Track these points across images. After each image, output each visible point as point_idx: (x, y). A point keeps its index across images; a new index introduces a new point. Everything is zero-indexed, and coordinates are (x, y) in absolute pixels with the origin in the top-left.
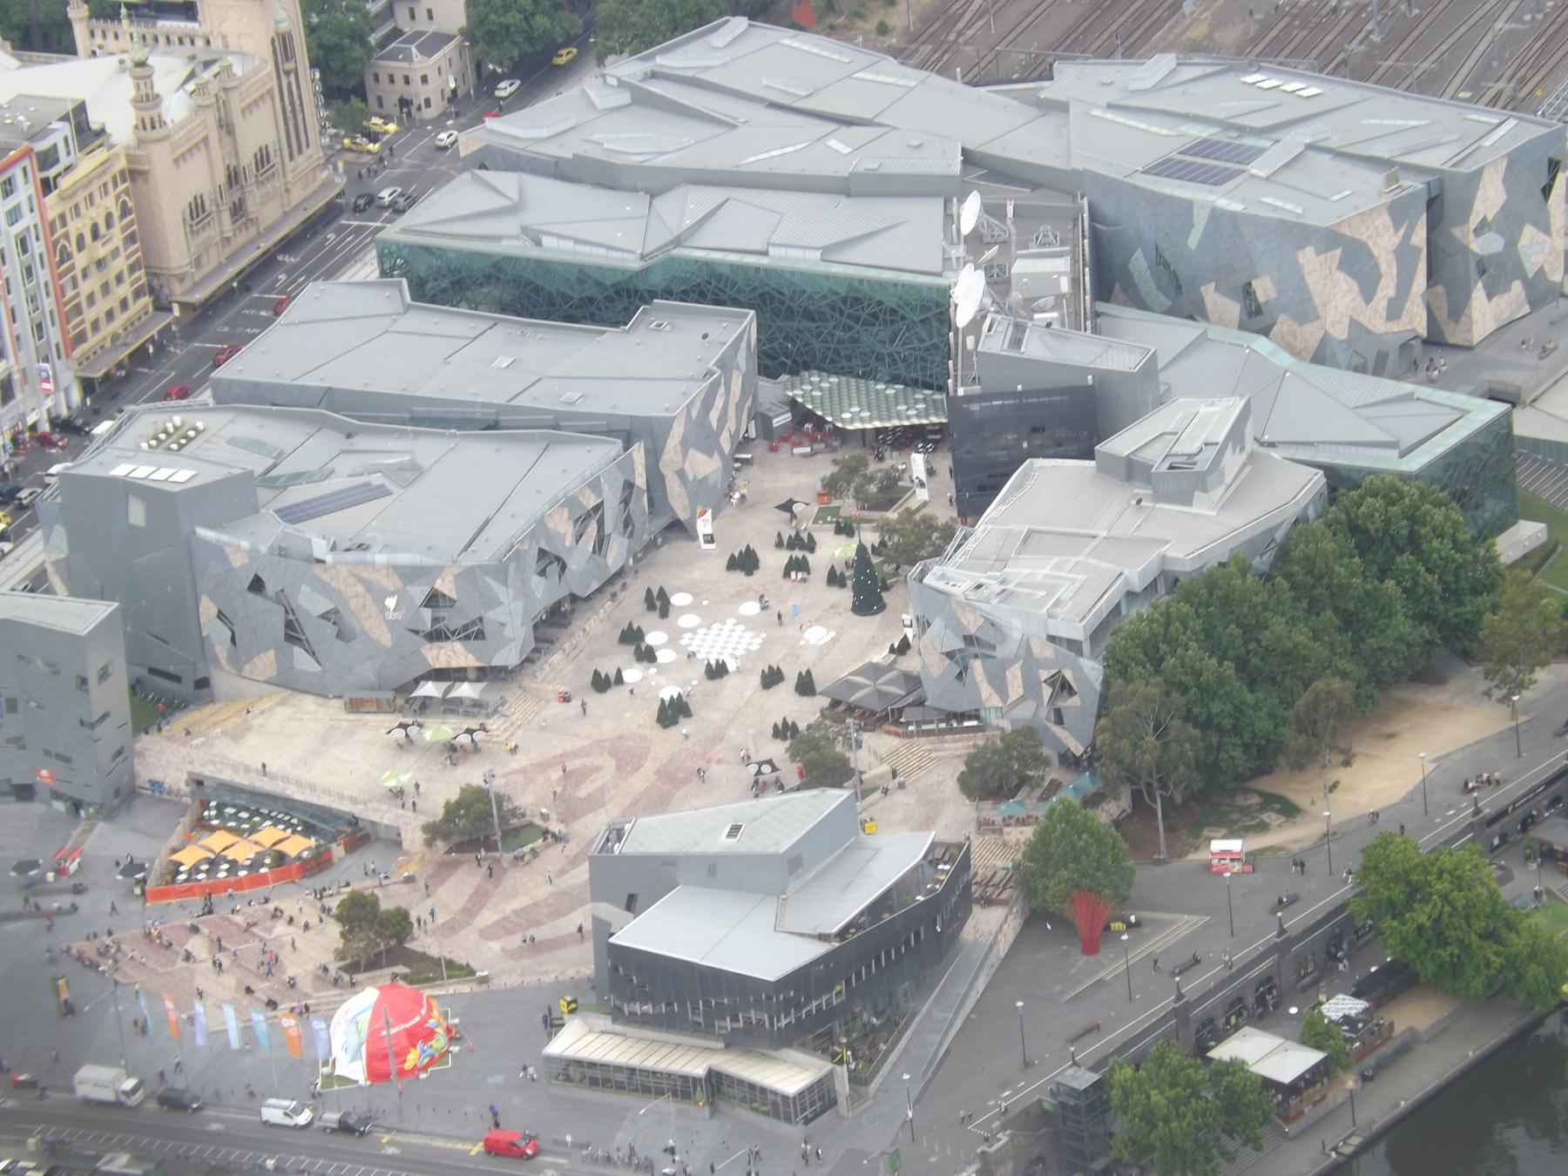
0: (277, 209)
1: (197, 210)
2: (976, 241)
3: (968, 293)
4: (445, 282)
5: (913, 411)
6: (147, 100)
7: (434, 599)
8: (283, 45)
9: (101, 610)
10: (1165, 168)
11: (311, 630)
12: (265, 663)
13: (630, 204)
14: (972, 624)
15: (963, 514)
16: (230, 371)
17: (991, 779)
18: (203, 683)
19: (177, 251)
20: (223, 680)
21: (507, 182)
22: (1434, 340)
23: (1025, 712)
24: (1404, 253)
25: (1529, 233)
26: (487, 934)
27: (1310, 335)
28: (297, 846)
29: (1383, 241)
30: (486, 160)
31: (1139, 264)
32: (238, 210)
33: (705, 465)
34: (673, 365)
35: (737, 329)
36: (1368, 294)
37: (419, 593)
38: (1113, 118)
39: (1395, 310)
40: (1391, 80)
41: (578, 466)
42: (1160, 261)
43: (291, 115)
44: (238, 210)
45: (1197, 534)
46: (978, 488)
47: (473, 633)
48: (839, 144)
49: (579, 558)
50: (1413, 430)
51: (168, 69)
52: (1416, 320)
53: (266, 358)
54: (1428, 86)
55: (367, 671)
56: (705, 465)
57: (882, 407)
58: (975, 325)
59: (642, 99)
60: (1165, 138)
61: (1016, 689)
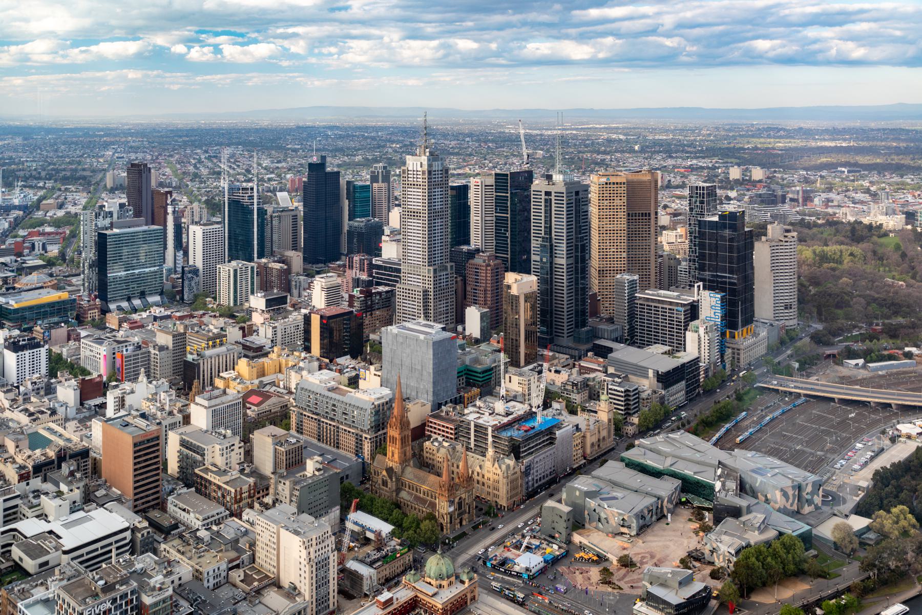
0: (605, 446)
1: (593, 445)
2: (720, 477)
3: (718, 485)
5: (706, 505)
7: (623, 519)
8: (609, 420)
9: (569, 509)
10: (753, 471)
11: (602, 520)
14: (715, 546)
15: (714, 524)
17: (715, 575)
19: (588, 451)
20: (587, 525)
21: (643, 450)
22: (798, 512)
23: (722, 564)
24: (794, 495)
25: (816, 497)
26: (626, 583)
27: (777, 506)
29: (790, 492)
31: (747, 486)
34: (666, 488)
36: (787, 499)
37: (621, 518)
38: (744, 461)
39: (792, 505)
40: (791, 463)
41: (650, 501)
42: (751, 487)
43: (609, 432)
45: (754, 537)
46: (717, 521)
47: (629, 527)
48: (698, 455)
49: (648, 518)
50: (795, 528)
52: (795, 508)
53: (600, 472)
54: (798, 466)
55: (610, 530)
56: (671, 506)
57: (700, 502)
58: (719, 491)
60: (753, 466)
61: (721, 560)
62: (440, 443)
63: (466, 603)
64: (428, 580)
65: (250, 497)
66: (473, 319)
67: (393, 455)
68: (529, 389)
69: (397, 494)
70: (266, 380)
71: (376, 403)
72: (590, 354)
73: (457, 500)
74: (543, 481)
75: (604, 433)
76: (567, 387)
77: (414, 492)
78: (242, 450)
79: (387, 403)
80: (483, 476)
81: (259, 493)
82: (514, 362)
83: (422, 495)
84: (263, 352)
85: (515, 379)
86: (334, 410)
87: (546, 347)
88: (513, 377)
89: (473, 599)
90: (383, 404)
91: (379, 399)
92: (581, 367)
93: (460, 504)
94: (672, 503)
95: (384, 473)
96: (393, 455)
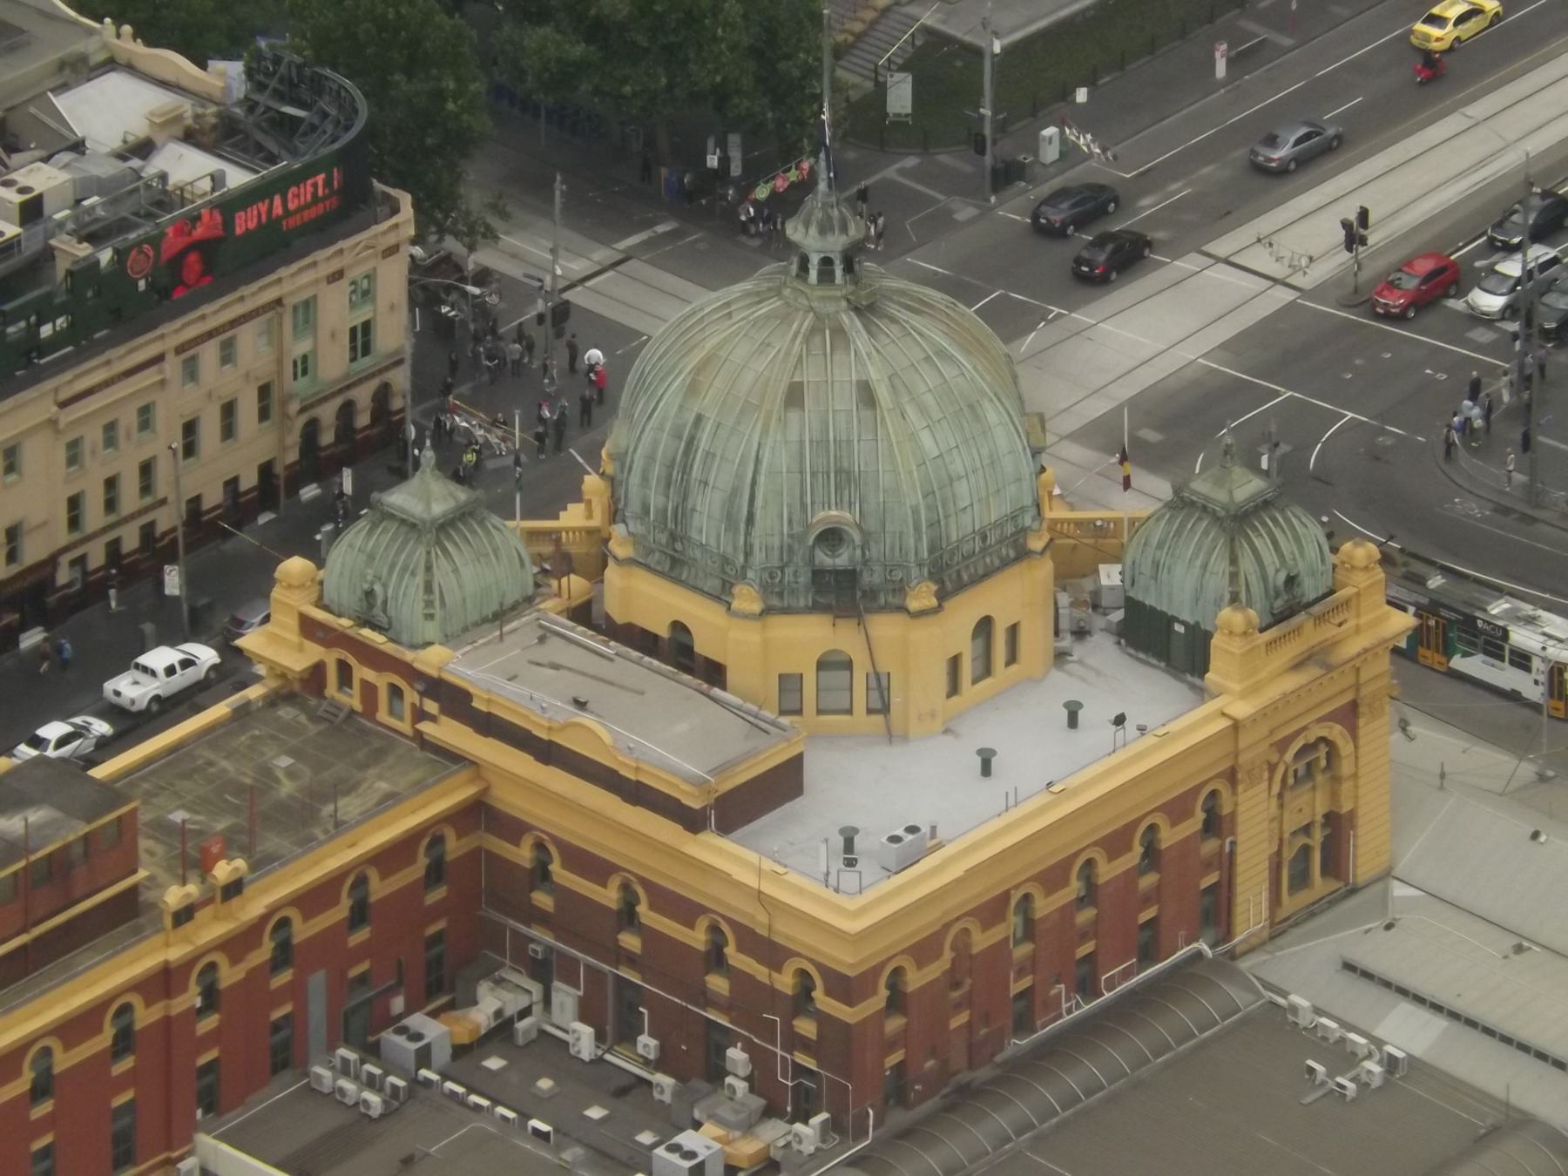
63: (1216, 911)
89: (1325, 861)
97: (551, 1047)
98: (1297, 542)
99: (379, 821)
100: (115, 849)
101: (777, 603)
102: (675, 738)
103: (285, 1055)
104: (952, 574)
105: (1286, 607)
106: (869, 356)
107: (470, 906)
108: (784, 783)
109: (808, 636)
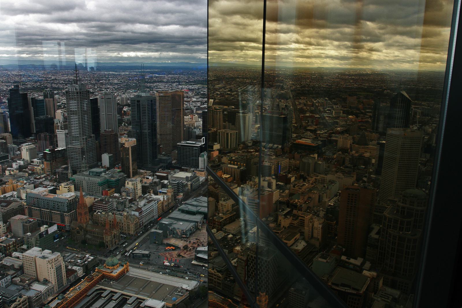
1: (166, 206)
4: (183, 211)
6: (164, 198)
8: (172, 195)
9: (162, 231)
12: (171, 236)
13: (195, 207)
16: (169, 216)
18: (167, 237)
19: (165, 208)
20: (169, 237)
28: (174, 248)
30: (185, 204)
32: (168, 206)
33: (200, 225)
35: (202, 216)
37: (182, 232)
43: (172, 200)
44: (168, 206)
47: (186, 235)
51: (165, 196)
56: (200, 225)
59: (195, 201)
62: (101, 213)
63: (125, 273)
64: (108, 267)
65: (14, 247)
66: (106, 158)
67: (81, 220)
68: (137, 186)
69: (85, 237)
70: (7, 195)
71: (69, 199)
72: (160, 170)
73: (113, 235)
74: (148, 222)
75: (170, 201)
76: (152, 184)
77: (93, 234)
78: (5, 227)
79: (74, 199)
80: (122, 224)
81: (18, 244)
82: (129, 177)
83: (96, 235)
84: (3, 182)
85: (130, 183)
86: (48, 205)
87: (141, 169)
88: (129, 182)
89: (128, 271)
90: (72, 199)
91: (70, 197)
92: (156, 175)
93: (114, 236)
94: (201, 223)
95: (78, 228)
96: (81, 220)
97: (106, 281)
98: (126, 262)
99: (100, 275)
100: (93, 277)
101: (111, 266)
102: (109, 271)
103: (98, 282)
104: (116, 265)
105: (126, 264)
106: (113, 259)
107: (103, 277)
108: (112, 272)
109: (112, 267)
